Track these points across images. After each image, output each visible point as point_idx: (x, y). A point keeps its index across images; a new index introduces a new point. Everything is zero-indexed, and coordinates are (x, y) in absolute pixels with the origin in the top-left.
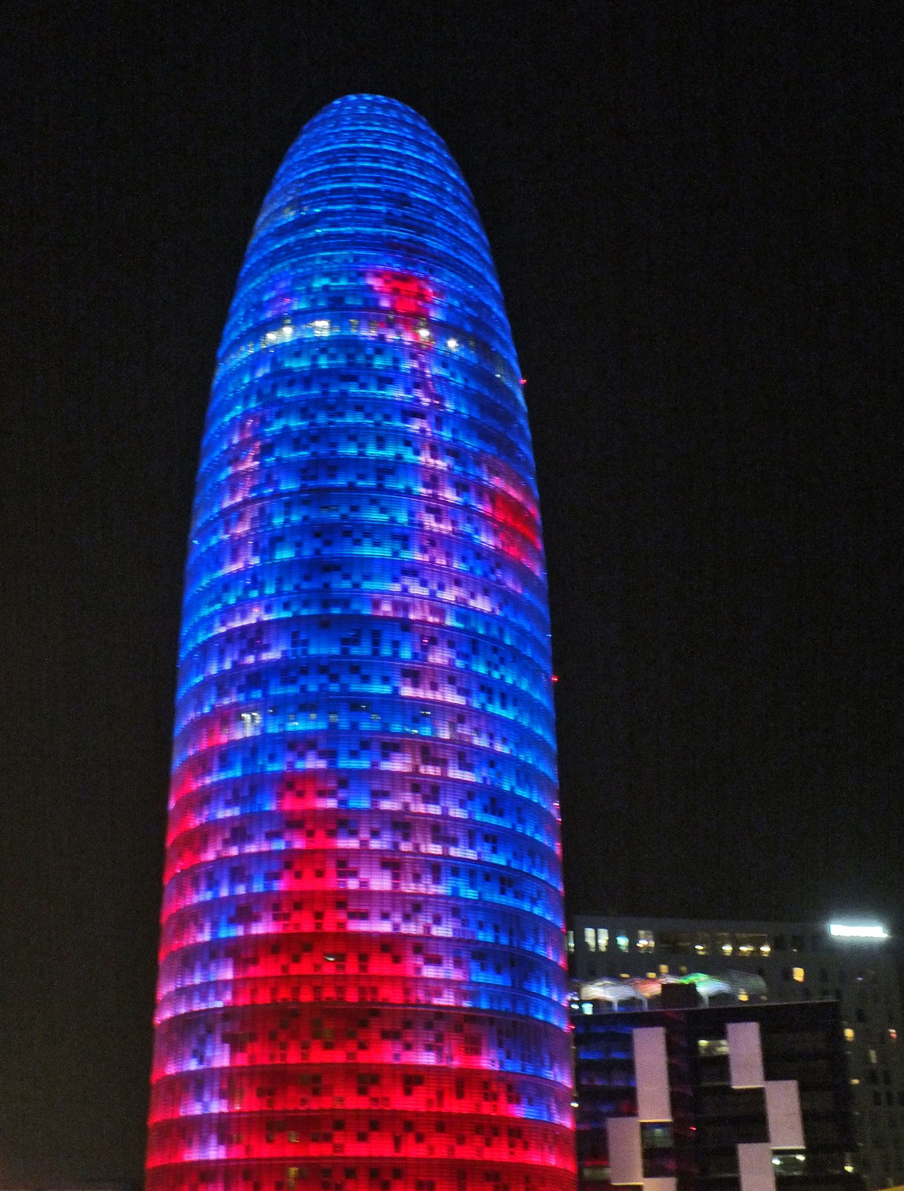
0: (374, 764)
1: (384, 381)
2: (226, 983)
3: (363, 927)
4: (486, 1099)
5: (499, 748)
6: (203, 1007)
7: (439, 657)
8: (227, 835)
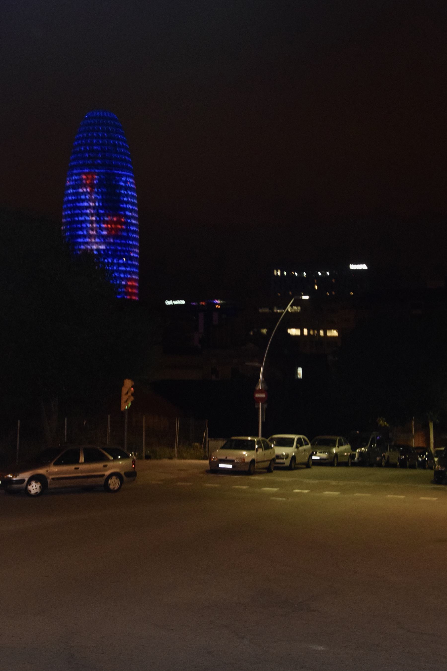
1: (83, 201)
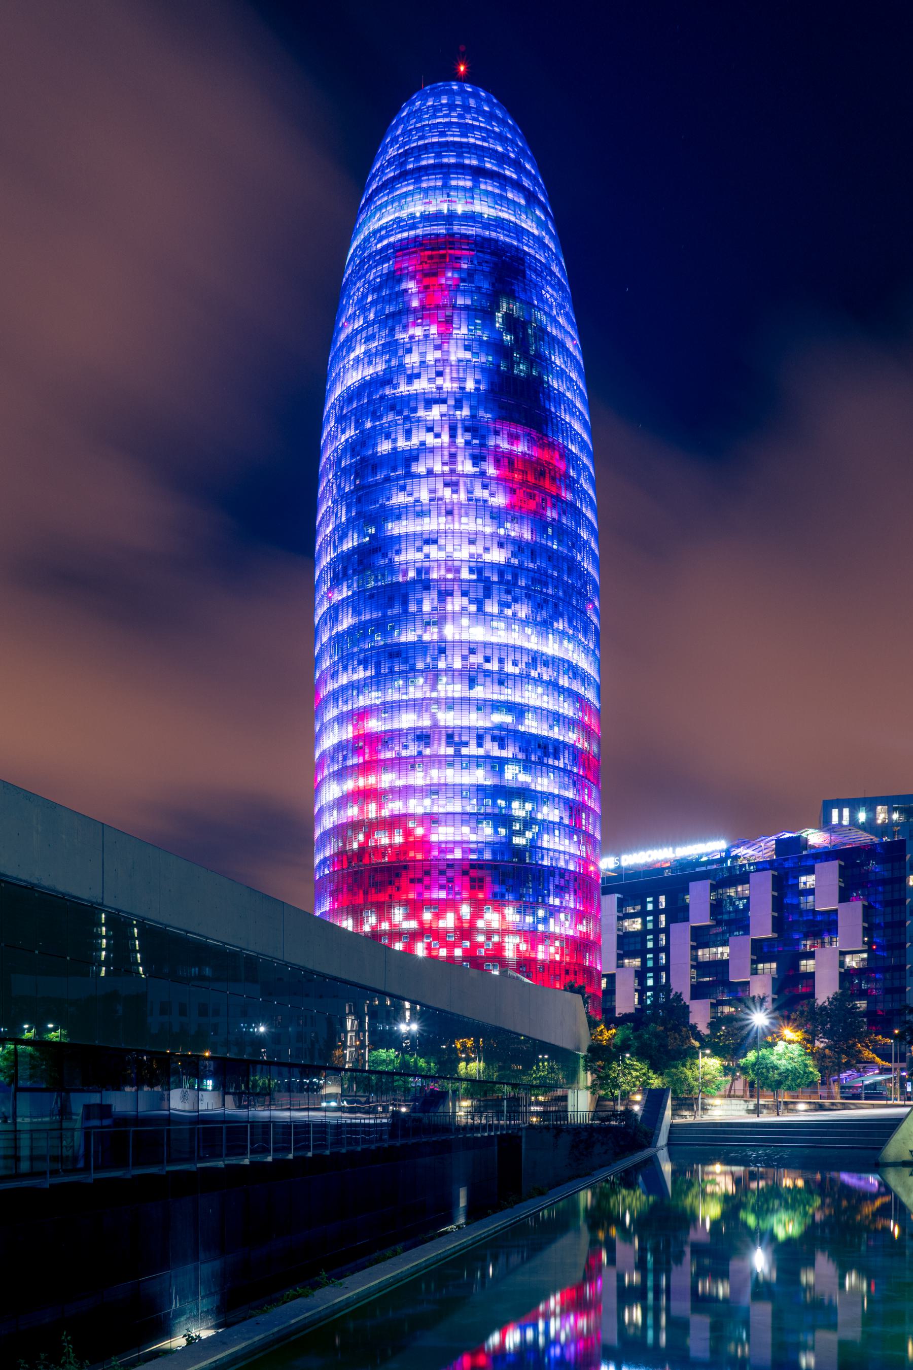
7: (455, 604)
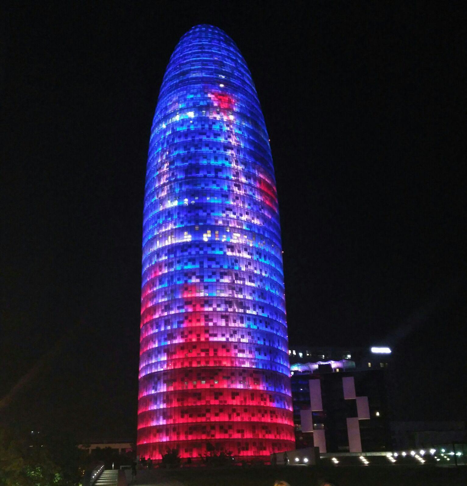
0: (218, 281)
1: (217, 135)
2: (164, 361)
3: (215, 339)
4: (262, 400)
5: (264, 274)
6: (156, 371)
8: (163, 308)
